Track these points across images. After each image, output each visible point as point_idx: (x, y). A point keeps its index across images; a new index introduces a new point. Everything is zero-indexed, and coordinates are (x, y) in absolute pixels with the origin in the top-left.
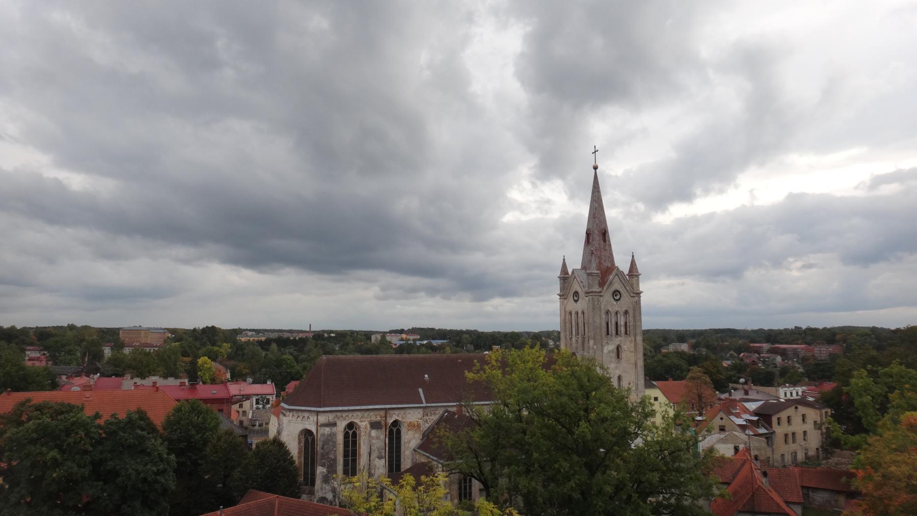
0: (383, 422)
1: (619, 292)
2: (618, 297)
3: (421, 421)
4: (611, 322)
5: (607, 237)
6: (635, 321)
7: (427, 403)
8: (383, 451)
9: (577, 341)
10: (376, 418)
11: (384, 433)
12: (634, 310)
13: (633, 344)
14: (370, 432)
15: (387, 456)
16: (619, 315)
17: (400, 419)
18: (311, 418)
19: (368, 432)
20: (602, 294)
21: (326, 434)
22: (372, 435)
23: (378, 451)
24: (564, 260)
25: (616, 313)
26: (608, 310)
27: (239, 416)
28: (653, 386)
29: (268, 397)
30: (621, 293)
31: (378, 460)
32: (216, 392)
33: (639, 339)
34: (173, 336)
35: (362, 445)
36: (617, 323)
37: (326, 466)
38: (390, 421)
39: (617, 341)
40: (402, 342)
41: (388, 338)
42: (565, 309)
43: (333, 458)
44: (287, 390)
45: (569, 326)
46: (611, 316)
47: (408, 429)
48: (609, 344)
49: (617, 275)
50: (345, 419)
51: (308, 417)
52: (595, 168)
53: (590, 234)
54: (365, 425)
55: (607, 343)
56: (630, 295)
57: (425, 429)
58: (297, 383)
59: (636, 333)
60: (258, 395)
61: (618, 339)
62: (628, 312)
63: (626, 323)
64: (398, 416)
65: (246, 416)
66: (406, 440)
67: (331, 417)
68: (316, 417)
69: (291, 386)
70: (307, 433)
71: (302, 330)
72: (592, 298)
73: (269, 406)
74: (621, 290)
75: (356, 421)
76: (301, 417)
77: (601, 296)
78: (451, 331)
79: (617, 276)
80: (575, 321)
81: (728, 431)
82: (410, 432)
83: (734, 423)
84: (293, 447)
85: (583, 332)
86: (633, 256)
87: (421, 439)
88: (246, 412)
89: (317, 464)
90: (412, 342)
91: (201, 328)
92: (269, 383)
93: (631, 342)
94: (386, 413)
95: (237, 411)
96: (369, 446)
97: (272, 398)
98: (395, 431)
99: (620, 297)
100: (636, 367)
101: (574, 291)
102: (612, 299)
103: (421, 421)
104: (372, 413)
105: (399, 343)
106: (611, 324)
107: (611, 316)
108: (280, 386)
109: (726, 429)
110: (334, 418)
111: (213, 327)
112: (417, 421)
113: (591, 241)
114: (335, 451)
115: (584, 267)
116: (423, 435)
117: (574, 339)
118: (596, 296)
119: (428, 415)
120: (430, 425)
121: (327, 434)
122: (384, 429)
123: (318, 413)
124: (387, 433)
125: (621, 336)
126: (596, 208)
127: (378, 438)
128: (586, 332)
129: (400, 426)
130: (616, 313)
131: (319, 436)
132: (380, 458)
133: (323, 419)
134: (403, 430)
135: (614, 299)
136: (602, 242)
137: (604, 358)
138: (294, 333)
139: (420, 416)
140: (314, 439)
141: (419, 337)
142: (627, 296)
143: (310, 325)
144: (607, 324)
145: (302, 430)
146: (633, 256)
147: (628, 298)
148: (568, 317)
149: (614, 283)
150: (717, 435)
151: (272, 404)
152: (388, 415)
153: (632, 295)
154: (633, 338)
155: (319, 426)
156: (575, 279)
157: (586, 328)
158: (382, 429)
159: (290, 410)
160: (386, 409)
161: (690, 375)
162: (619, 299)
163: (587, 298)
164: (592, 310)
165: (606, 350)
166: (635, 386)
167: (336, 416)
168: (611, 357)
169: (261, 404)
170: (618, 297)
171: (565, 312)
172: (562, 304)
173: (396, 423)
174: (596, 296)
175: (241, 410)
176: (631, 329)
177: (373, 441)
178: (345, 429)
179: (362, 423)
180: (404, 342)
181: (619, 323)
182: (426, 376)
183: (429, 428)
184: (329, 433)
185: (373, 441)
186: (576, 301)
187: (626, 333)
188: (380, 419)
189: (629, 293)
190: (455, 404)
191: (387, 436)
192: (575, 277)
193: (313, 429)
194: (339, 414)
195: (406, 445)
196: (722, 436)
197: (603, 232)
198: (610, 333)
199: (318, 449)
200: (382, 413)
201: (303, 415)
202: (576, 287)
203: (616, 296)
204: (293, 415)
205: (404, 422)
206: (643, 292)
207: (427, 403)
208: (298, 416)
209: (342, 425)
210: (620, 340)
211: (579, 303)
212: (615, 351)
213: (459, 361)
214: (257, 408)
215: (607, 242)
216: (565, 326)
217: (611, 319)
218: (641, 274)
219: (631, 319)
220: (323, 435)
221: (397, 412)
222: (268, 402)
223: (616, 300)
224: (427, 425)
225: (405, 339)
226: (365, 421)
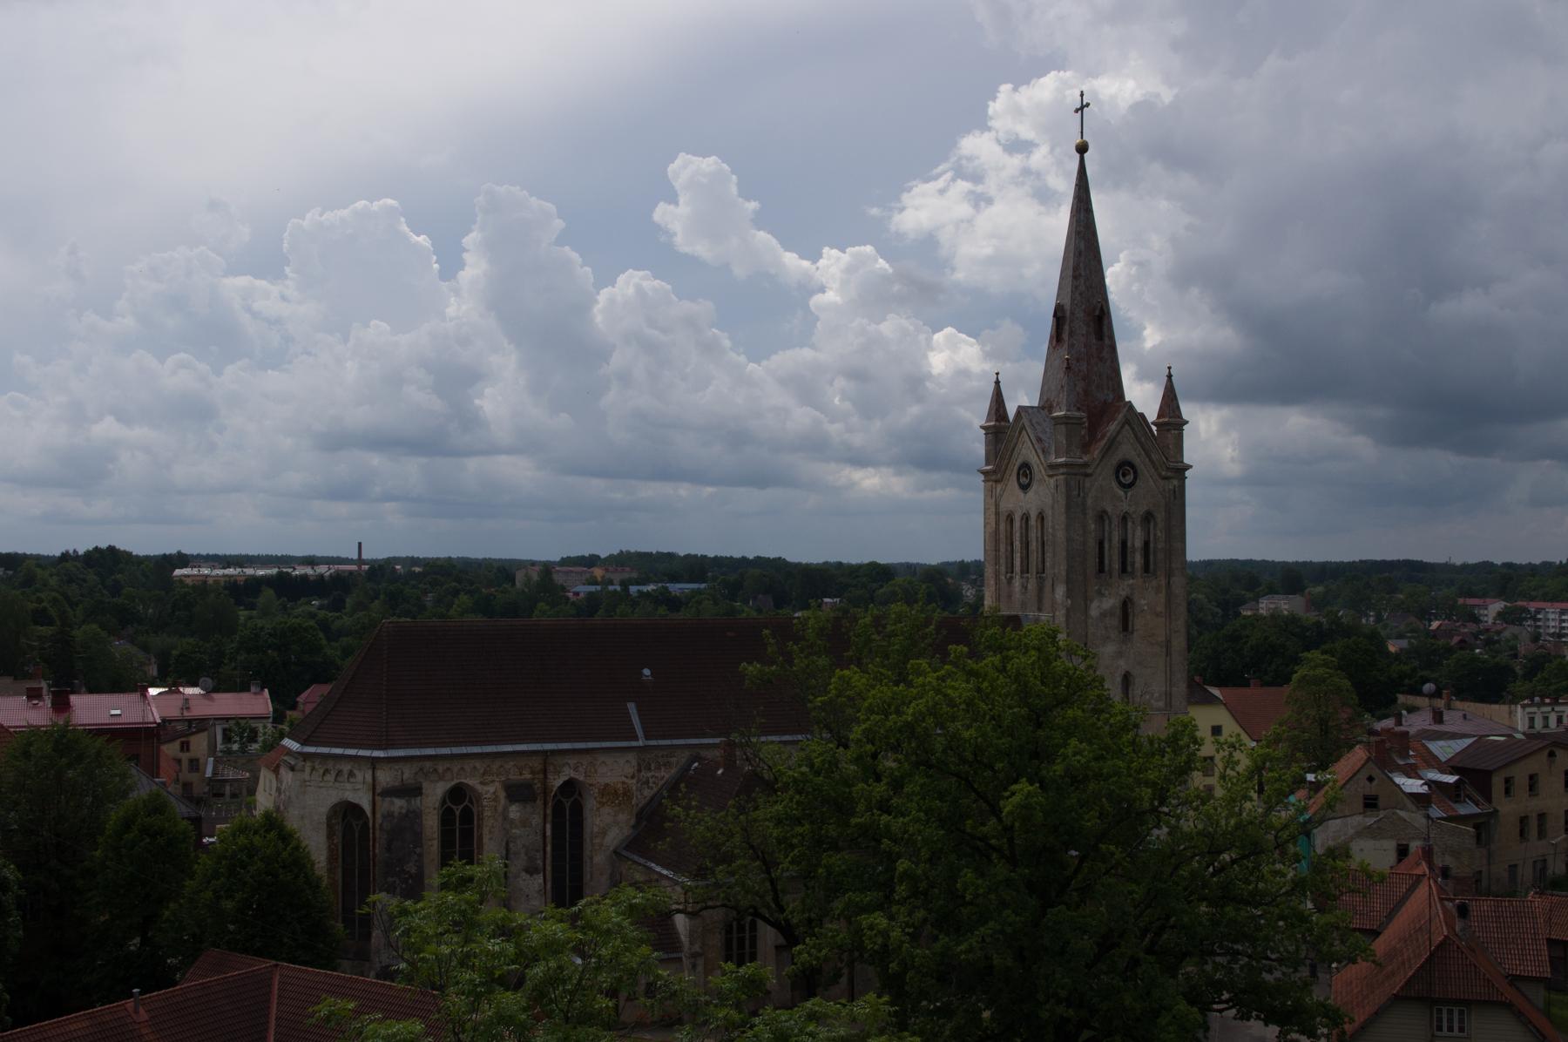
0: (539, 785)
2: (1130, 478)
3: (634, 781)
4: (1110, 540)
5: (1105, 329)
7: (647, 738)
8: (539, 855)
9: (1024, 587)
10: (521, 774)
11: (542, 812)
14: (505, 809)
15: (549, 868)
16: (1130, 524)
17: (581, 778)
18: (359, 776)
19: (500, 809)
20: (1089, 471)
21: (396, 814)
22: (512, 815)
23: (526, 854)
24: (997, 382)
26: (1105, 512)
27: (181, 770)
28: (1210, 700)
29: (254, 725)
30: (1139, 471)
31: (528, 876)
32: (118, 712)
33: (1178, 582)
34: (10, 572)
35: (486, 840)
36: (1124, 544)
37: (398, 890)
38: (557, 782)
39: (1123, 588)
40: (592, 588)
41: (558, 579)
42: (997, 506)
43: (413, 871)
44: (301, 707)
45: (1006, 550)
46: (1110, 526)
47: (600, 803)
49: (1127, 422)
50: (442, 778)
51: (351, 774)
52: (1082, 149)
53: (1064, 317)
54: (494, 793)
55: (1100, 594)
56: (1160, 475)
57: (643, 802)
58: (324, 689)
60: (227, 719)
61: (1126, 583)
63: (1146, 544)
64: (576, 769)
65: (197, 770)
66: (596, 829)
67: (408, 773)
68: (370, 772)
69: (311, 697)
70: (347, 813)
71: (338, 558)
72: (1067, 485)
73: (255, 746)
74: (1137, 461)
75: (470, 782)
76: (333, 774)
78: (718, 562)
79: (1127, 427)
80: (1021, 536)
81: (1384, 809)
82: (606, 810)
83: (1401, 789)
84: (316, 845)
85: (1040, 566)
87: (633, 827)
88: (197, 760)
89: (374, 886)
90: (618, 588)
91: (81, 552)
92: (253, 689)
94: (545, 763)
95: (174, 759)
96: (504, 844)
97: (265, 727)
98: (568, 805)
99: (1135, 478)
100: (1168, 653)
101: (1019, 461)
102: (1114, 484)
103: (634, 781)
104: (512, 763)
105: (584, 589)
106: (1110, 546)
107: (1110, 526)
108: (284, 700)
109: (1381, 803)
110: (416, 773)
111: (111, 549)
112: (623, 783)
113: (1065, 336)
114: (420, 855)
115: (1046, 406)
116: (639, 817)
117: (1017, 583)
118: (1076, 474)
119: (650, 769)
120: (655, 790)
121: (400, 813)
122: (539, 802)
123: (374, 763)
124: (549, 811)
125: (1132, 575)
126: (1080, 254)
127: (525, 823)
128: (1047, 564)
129: (580, 795)
130: (1124, 519)
131: (379, 820)
132: (531, 870)
133: (385, 777)
134: (590, 804)
135: (1120, 483)
138: (318, 564)
139: (630, 770)
140: (366, 824)
141: (635, 575)
143: (360, 544)
144: (1101, 544)
145: (336, 805)
148: (1002, 527)
150: (1359, 818)
151: (264, 741)
152: (551, 768)
153: (1163, 473)
154: (1163, 583)
155: (379, 795)
156: (1024, 432)
157: (1048, 555)
158: (535, 801)
159: (306, 757)
160: (545, 752)
161: (1301, 671)
163: (1052, 481)
164: (1063, 510)
165: (1094, 611)
166: (1164, 697)
167: (421, 769)
168: (1106, 628)
169: (235, 742)
170: (1130, 478)
171: (997, 514)
172: (989, 493)
173: (570, 786)
174: (1076, 474)
175: (185, 757)
177: (514, 831)
178: (444, 802)
179: (486, 788)
180: (599, 588)
181: (1129, 544)
182: (647, 672)
183: (652, 799)
184: (404, 811)
185: (514, 831)
186: (1025, 488)
187: (1146, 568)
188: (529, 776)
189: (1156, 469)
190: (717, 740)
191: (549, 818)
192: (1023, 428)
193: (365, 803)
194: (428, 764)
195: (597, 841)
196: (1370, 821)
197: (1097, 313)
198: (1106, 569)
199: (377, 851)
200: (536, 763)
201: (338, 767)
202: (1027, 451)
203: (1124, 475)
204: (313, 769)
205: (591, 785)
206: (1191, 467)
207: (647, 738)
208: (326, 771)
209: (435, 792)
210: (1132, 585)
211: (1031, 493)
212: (1118, 612)
213: (729, 634)
214: (229, 752)
215: (1107, 341)
216: (997, 550)
217: (1110, 533)
218: (1187, 422)
219: (1159, 534)
220: (389, 815)
221: (572, 762)
222: (253, 737)
224: (648, 793)
225: (599, 579)
226: (493, 781)
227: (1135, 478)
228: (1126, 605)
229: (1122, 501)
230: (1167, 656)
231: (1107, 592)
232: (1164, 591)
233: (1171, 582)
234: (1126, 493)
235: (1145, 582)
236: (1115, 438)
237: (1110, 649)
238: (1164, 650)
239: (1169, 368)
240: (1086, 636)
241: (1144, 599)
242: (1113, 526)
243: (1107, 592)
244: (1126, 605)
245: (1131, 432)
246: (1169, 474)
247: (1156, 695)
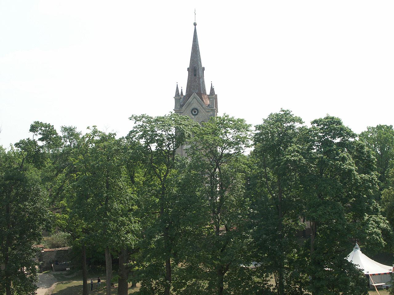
1: (197, 110)
2: (196, 113)
20: (182, 112)
49: (195, 98)
52: (195, 24)
56: (206, 111)
74: (198, 108)
79: (195, 99)
86: (212, 84)
99: (198, 113)
102: (191, 114)
135: (193, 114)
142: (204, 112)
147: (204, 113)
149: (193, 104)
162: (196, 115)
170: (196, 113)
203: (195, 112)
215: (197, 76)
223: (194, 115)
227: (198, 113)
234: (195, 117)
240: (182, 154)
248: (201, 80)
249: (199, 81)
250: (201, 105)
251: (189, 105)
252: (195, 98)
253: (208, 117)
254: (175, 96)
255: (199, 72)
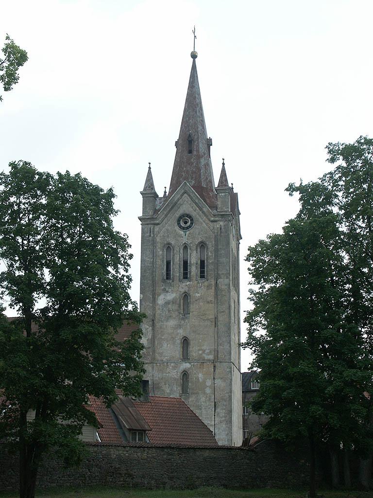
1: (190, 217)
2: (189, 224)
6: (217, 256)
12: (217, 241)
13: (212, 291)
20: (157, 222)
25: (185, 247)
36: (185, 264)
39: (184, 286)
48: (167, 292)
49: (185, 192)
52: (194, 56)
55: (164, 290)
59: (217, 273)
62: (206, 244)
63: (202, 263)
77: (158, 224)
86: (223, 164)
93: (209, 287)
99: (192, 223)
102: (177, 228)
106: (173, 263)
135: (180, 227)
136: (186, 153)
137: (158, 312)
144: (168, 263)
146: (223, 164)
153: (212, 219)
154: (213, 283)
162: (187, 228)
165: (161, 300)
168: (169, 311)
170: (189, 224)
174: (148, 224)
176: (209, 268)
181: (188, 262)
187: (202, 277)
189: (206, 216)
203: (186, 223)
215: (195, 153)
217: (174, 255)
223: (183, 228)
227: (192, 223)
228: (186, 296)
229: (182, 237)
230: (215, 327)
231: (170, 290)
232: (213, 288)
233: (218, 282)
235: (198, 283)
236: (176, 203)
237: (172, 323)
238: (214, 323)
239: (223, 160)
240: (155, 315)
241: (198, 293)
242: (175, 251)
243: (170, 290)
244: (186, 296)
245: (189, 198)
246: (217, 219)
247: (207, 351)
248: (203, 161)
249: (198, 163)
250: (198, 206)
251: (172, 208)
252: (185, 192)
253: (213, 233)
254: (145, 189)
255: (198, 146)
